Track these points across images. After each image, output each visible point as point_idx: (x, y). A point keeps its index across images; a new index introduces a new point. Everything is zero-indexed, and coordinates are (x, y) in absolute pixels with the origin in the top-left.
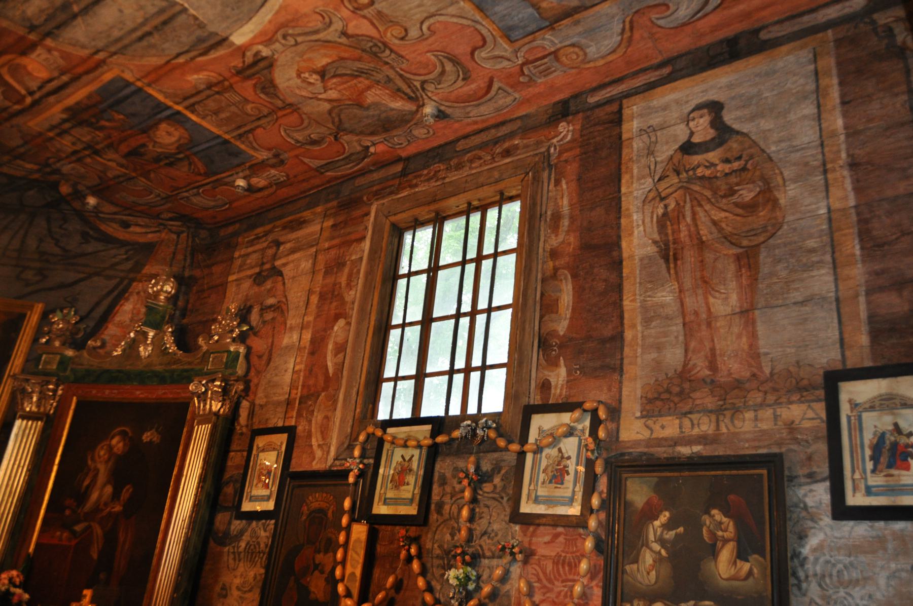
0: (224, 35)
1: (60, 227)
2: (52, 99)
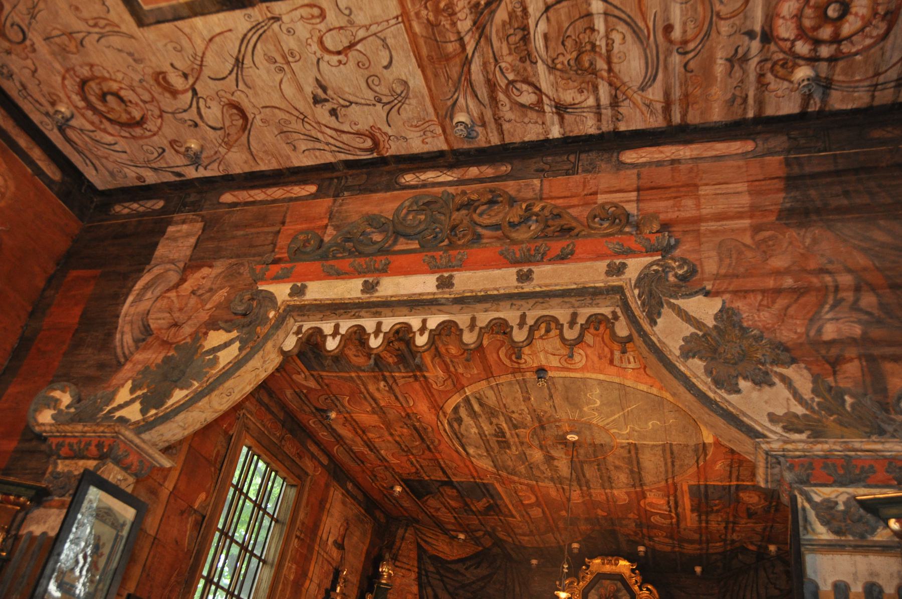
0: (701, 442)
1: (773, 573)
2: (680, 510)
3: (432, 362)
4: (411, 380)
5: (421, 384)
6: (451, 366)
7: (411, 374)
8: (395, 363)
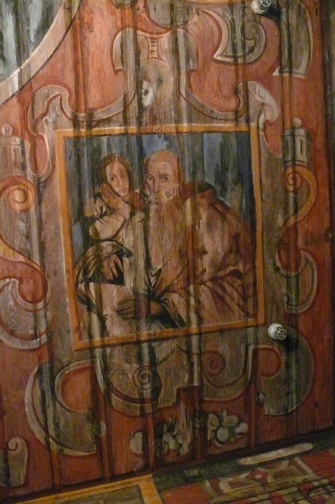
3: (54, 166)
4: (99, 115)
5: (86, 103)
6: (27, 156)
7: (95, 130)
8: (110, 159)
